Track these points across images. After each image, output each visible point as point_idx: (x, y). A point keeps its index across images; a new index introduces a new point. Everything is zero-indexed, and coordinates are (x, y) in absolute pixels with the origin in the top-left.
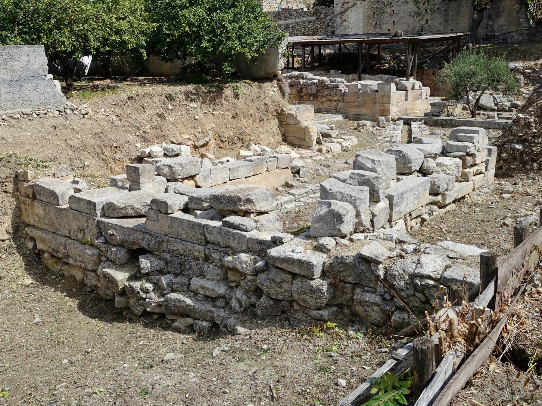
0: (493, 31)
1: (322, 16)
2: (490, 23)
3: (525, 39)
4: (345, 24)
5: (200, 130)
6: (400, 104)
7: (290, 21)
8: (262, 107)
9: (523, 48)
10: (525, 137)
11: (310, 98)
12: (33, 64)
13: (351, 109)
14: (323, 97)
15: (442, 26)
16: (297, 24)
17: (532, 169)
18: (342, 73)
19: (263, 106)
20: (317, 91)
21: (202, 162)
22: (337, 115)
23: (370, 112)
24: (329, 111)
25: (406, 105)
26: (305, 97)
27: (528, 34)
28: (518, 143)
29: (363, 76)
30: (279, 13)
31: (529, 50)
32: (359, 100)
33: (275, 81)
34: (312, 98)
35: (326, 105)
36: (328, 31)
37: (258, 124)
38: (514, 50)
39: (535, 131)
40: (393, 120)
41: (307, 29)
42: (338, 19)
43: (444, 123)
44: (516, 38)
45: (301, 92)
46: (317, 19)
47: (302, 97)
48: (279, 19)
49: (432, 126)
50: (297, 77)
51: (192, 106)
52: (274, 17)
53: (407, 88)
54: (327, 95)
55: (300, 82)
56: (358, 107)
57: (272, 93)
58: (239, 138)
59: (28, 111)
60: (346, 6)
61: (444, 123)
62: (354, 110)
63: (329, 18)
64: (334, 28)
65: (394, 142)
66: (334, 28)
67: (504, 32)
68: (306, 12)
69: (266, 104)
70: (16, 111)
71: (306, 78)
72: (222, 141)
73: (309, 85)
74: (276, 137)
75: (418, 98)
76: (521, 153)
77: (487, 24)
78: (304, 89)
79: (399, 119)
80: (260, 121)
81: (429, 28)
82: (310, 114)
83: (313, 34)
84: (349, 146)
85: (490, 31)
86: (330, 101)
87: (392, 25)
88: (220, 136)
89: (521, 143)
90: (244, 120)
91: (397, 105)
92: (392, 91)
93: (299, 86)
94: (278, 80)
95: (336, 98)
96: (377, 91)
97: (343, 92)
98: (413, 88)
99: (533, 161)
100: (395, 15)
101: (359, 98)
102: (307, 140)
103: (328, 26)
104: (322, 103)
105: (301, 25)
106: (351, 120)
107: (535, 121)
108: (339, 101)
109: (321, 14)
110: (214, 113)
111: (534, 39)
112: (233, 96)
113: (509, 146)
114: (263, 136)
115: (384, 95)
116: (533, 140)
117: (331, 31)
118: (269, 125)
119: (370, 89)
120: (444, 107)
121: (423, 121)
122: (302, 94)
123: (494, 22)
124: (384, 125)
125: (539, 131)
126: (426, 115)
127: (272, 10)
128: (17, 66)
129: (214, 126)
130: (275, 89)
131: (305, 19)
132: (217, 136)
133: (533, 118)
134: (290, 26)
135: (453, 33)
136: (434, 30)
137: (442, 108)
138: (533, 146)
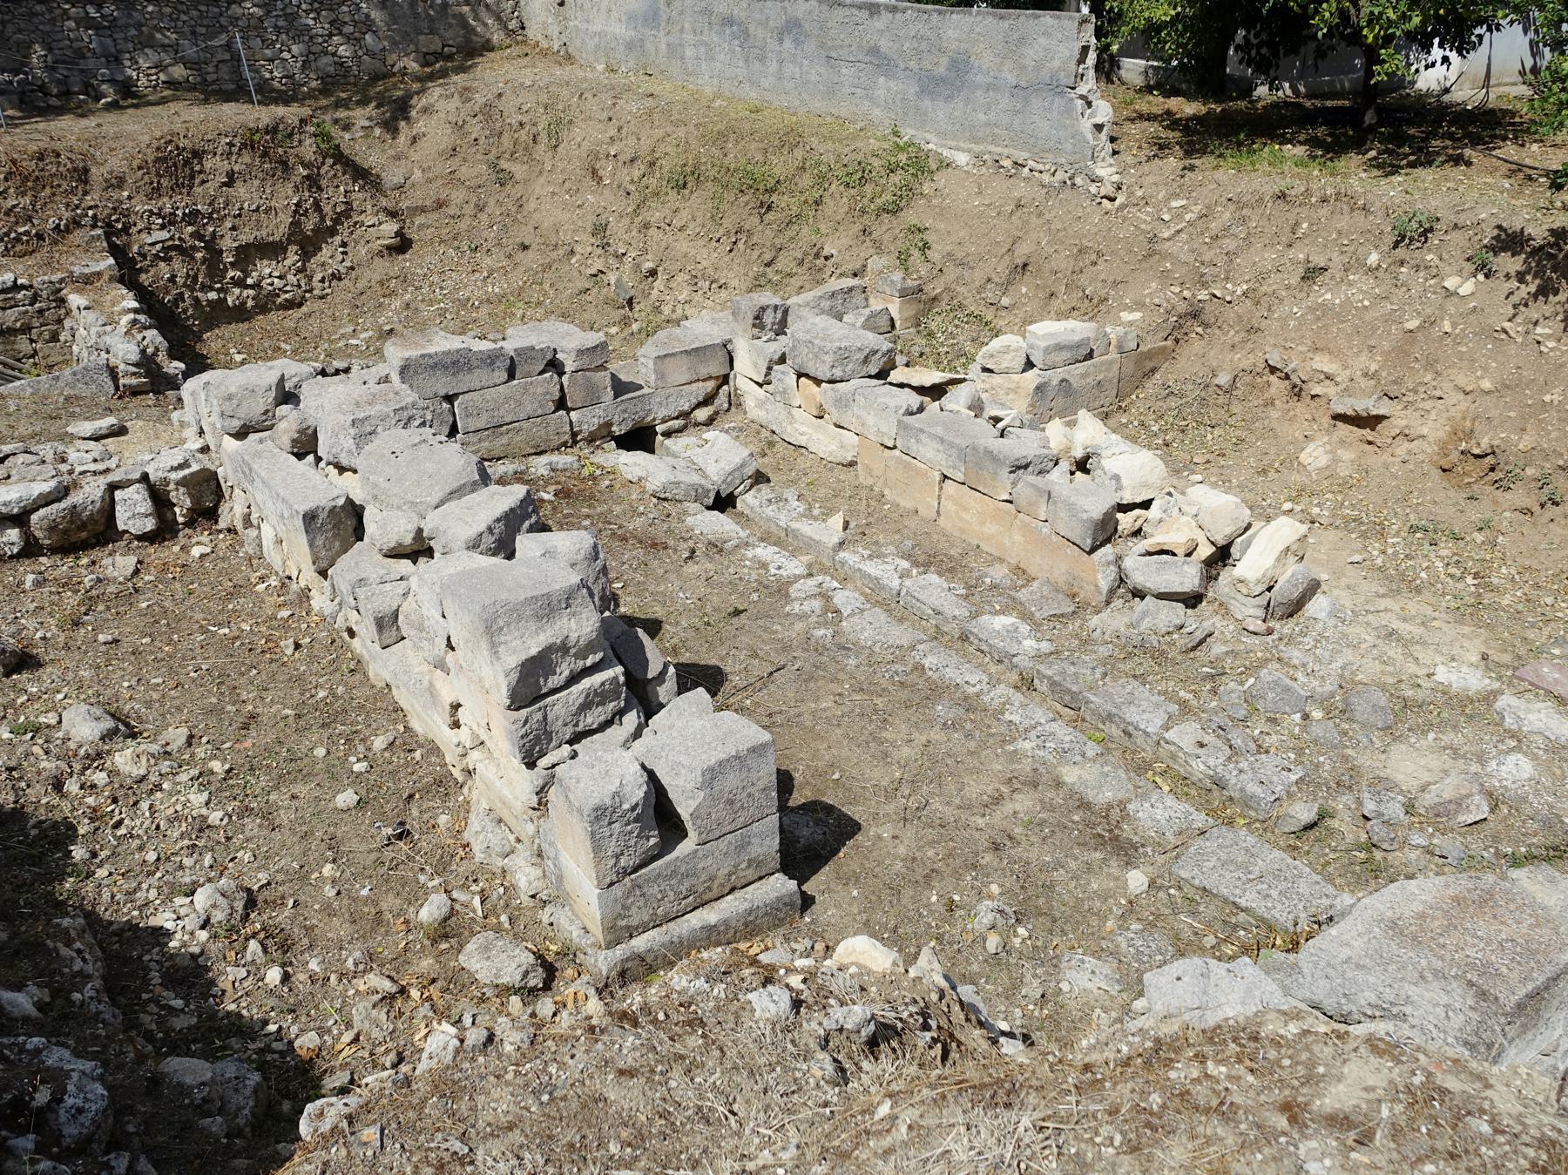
12: (1052, 58)
51: (1450, 283)
59: (1021, 156)
70: (1006, 151)
128: (1030, 54)
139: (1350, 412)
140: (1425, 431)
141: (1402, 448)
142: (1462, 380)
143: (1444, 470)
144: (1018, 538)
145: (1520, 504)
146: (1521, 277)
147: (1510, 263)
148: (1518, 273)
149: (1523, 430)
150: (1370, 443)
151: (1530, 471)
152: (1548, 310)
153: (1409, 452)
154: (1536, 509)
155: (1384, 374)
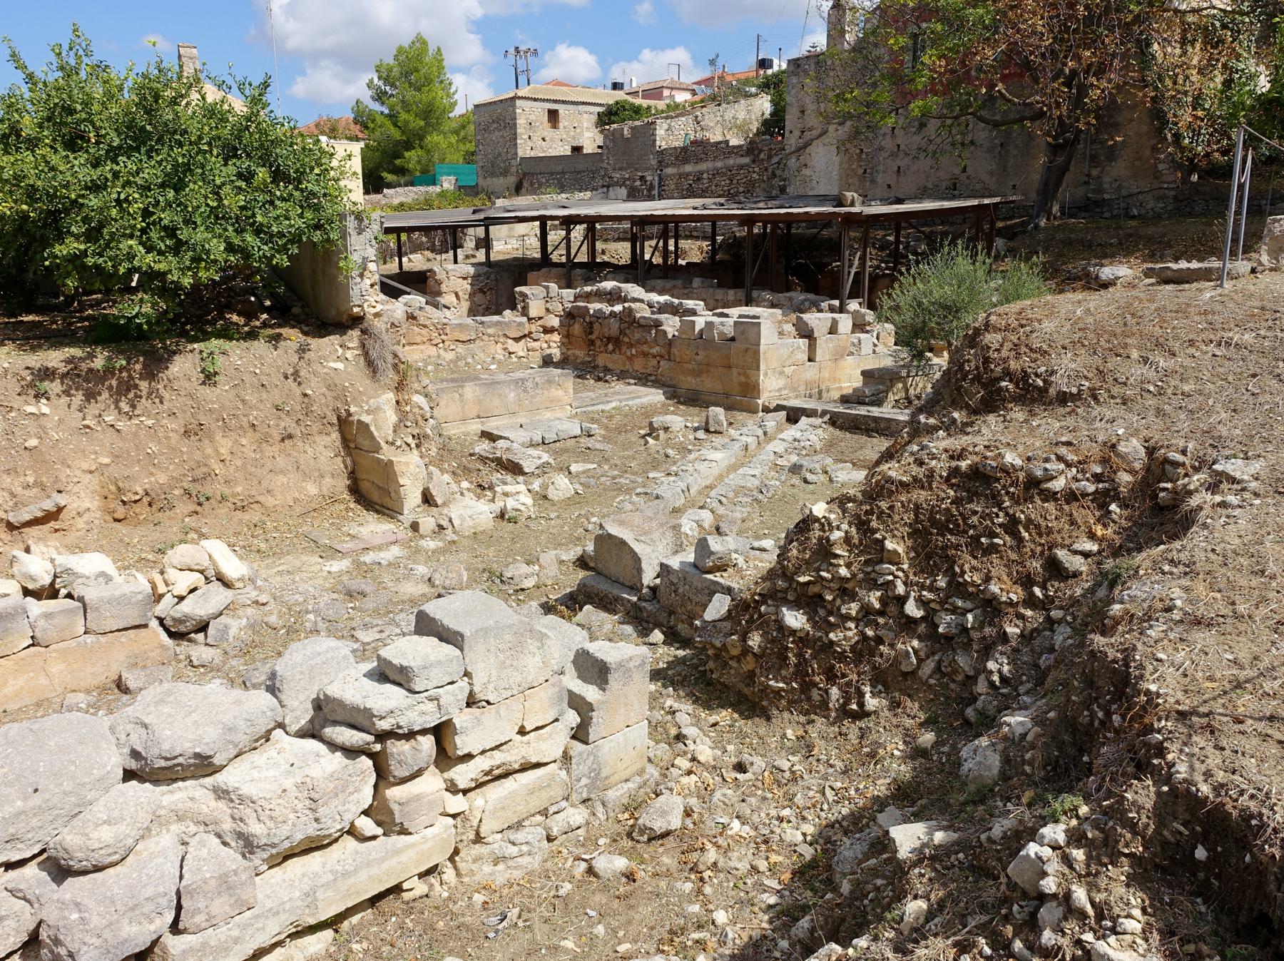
0: (1099, 190)
1: (762, 156)
2: (1095, 173)
3: (1169, 208)
4: (806, 172)
5: (31, 480)
6: (788, 370)
7: (703, 166)
8: (295, 404)
9: (1151, 230)
10: (815, 589)
13: (682, 378)
14: (631, 346)
15: (994, 179)
16: (716, 173)
17: (822, 707)
18: (720, 286)
19: (300, 398)
20: (622, 332)
21: (52, 561)
22: (653, 390)
23: (718, 387)
24: (644, 380)
25: (810, 372)
26: (598, 343)
27: (1175, 198)
28: (796, 605)
29: (755, 294)
30: (684, 149)
31: (1164, 235)
32: (698, 358)
33: (355, 333)
34: (610, 347)
35: (638, 365)
36: (772, 187)
37: (276, 448)
38: (1131, 235)
39: (843, 572)
40: (767, 410)
42: (792, 162)
43: (873, 425)
44: (1149, 206)
45: (591, 333)
46: (754, 161)
47: (592, 343)
48: (686, 161)
49: (847, 430)
50: (610, 293)
51: (30, 409)
52: (677, 159)
53: (812, 331)
54: (639, 342)
55: (587, 309)
56: (697, 373)
57: (340, 366)
58: (187, 493)
60: (808, 135)
61: (873, 425)
62: (689, 379)
63: (775, 160)
65: (657, 497)
67: (1124, 193)
68: (734, 147)
69: (305, 395)
71: (625, 300)
72: (124, 503)
74: (328, 480)
75: (852, 354)
76: (803, 640)
77: (1088, 175)
78: (596, 326)
79: (779, 408)
80: (283, 440)
81: (967, 182)
82: (560, 393)
83: (690, 194)
84: (522, 508)
85: (1094, 191)
86: (645, 355)
87: (895, 176)
88: (119, 489)
89: (808, 605)
90: (224, 441)
91: (782, 373)
92: (762, 341)
93: (587, 319)
94: (364, 332)
95: (655, 350)
96: (733, 339)
97: (670, 336)
98: (833, 330)
99: (831, 677)
100: (901, 156)
102: (393, 494)
103: (774, 175)
104: (630, 359)
105: (725, 174)
106: (681, 403)
107: (847, 540)
108: (662, 357)
109: (761, 151)
110: (120, 425)
111: (1188, 209)
112: (196, 375)
113: (772, 609)
114: (282, 479)
115: (747, 350)
116: (838, 602)
118: (309, 450)
119: (721, 333)
120: (891, 380)
121: (828, 416)
122: (593, 337)
123: (1102, 172)
124: (718, 428)
125: (854, 576)
126: (845, 400)
127: (676, 144)
129: (106, 460)
130: (349, 354)
131: (731, 162)
132: (113, 488)
133: (845, 527)
134: (705, 176)
135: (953, 198)
136: (978, 187)
137: (888, 383)
138: (832, 627)
139: (39, 514)
140: (88, 505)
141: (80, 523)
142: (85, 466)
143: (119, 521)
144: (56, 668)
145: (186, 512)
146: (67, 393)
147: (55, 387)
148: (64, 392)
149: (152, 474)
150: (56, 531)
151: (177, 492)
152: (101, 406)
153: (87, 523)
154: (199, 509)
155: (44, 479)
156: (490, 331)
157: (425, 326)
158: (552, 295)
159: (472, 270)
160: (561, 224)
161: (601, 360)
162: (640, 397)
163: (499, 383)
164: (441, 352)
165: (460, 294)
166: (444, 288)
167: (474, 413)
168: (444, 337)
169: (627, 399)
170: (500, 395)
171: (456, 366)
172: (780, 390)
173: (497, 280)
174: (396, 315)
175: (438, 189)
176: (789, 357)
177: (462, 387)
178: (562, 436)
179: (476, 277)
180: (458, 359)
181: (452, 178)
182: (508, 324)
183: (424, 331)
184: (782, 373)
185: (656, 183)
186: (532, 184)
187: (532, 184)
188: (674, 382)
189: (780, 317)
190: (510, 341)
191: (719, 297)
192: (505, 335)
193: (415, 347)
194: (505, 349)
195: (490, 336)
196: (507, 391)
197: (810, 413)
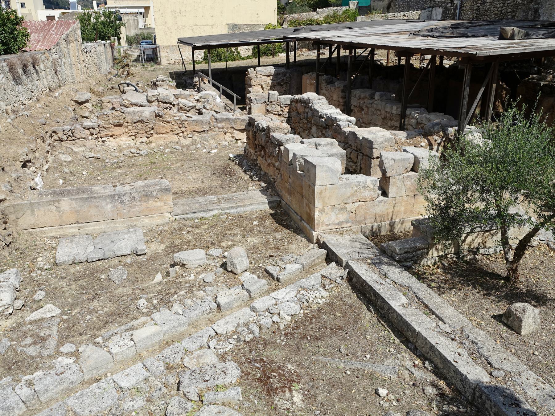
11: (261, 151)
13: (284, 192)
34: (263, 153)
36: (529, 9)
41: (506, 5)
43: (373, 298)
45: (255, 140)
56: (291, 193)
61: (373, 298)
64: (538, 4)
66: (538, 4)
73: (260, 131)
79: (323, 245)
82: (159, 204)
92: (318, 182)
101: (290, 177)
117: (534, 8)
137: (430, 241)
156: (220, 125)
157: (168, 122)
158: (271, 100)
159: (272, 70)
160: (313, 44)
161: (260, 161)
162: (244, 206)
163: (95, 198)
164: (181, 138)
165: (264, 86)
166: (253, 82)
167: (73, 220)
168: (183, 129)
169: (230, 208)
170: (97, 207)
171: (188, 149)
172: (341, 223)
173: (290, 77)
174: (144, 115)
175: (344, 8)
176: (353, 195)
177: (58, 201)
178: (108, 254)
179: (276, 75)
180: (193, 144)
181: (356, 2)
182: (234, 120)
183: (167, 125)
184: (343, 209)
185: (458, 5)
186: (395, 5)
187: (395, 5)
188: (281, 194)
189: (403, 140)
190: (236, 132)
191: (388, 110)
192: (233, 128)
193: (161, 135)
194: (233, 137)
195: (219, 128)
196: (104, 203)
197: (339, 263)
